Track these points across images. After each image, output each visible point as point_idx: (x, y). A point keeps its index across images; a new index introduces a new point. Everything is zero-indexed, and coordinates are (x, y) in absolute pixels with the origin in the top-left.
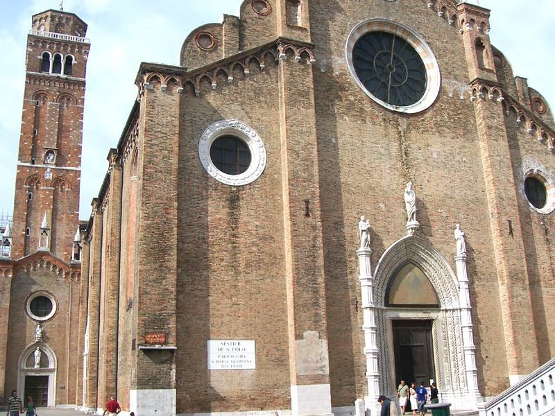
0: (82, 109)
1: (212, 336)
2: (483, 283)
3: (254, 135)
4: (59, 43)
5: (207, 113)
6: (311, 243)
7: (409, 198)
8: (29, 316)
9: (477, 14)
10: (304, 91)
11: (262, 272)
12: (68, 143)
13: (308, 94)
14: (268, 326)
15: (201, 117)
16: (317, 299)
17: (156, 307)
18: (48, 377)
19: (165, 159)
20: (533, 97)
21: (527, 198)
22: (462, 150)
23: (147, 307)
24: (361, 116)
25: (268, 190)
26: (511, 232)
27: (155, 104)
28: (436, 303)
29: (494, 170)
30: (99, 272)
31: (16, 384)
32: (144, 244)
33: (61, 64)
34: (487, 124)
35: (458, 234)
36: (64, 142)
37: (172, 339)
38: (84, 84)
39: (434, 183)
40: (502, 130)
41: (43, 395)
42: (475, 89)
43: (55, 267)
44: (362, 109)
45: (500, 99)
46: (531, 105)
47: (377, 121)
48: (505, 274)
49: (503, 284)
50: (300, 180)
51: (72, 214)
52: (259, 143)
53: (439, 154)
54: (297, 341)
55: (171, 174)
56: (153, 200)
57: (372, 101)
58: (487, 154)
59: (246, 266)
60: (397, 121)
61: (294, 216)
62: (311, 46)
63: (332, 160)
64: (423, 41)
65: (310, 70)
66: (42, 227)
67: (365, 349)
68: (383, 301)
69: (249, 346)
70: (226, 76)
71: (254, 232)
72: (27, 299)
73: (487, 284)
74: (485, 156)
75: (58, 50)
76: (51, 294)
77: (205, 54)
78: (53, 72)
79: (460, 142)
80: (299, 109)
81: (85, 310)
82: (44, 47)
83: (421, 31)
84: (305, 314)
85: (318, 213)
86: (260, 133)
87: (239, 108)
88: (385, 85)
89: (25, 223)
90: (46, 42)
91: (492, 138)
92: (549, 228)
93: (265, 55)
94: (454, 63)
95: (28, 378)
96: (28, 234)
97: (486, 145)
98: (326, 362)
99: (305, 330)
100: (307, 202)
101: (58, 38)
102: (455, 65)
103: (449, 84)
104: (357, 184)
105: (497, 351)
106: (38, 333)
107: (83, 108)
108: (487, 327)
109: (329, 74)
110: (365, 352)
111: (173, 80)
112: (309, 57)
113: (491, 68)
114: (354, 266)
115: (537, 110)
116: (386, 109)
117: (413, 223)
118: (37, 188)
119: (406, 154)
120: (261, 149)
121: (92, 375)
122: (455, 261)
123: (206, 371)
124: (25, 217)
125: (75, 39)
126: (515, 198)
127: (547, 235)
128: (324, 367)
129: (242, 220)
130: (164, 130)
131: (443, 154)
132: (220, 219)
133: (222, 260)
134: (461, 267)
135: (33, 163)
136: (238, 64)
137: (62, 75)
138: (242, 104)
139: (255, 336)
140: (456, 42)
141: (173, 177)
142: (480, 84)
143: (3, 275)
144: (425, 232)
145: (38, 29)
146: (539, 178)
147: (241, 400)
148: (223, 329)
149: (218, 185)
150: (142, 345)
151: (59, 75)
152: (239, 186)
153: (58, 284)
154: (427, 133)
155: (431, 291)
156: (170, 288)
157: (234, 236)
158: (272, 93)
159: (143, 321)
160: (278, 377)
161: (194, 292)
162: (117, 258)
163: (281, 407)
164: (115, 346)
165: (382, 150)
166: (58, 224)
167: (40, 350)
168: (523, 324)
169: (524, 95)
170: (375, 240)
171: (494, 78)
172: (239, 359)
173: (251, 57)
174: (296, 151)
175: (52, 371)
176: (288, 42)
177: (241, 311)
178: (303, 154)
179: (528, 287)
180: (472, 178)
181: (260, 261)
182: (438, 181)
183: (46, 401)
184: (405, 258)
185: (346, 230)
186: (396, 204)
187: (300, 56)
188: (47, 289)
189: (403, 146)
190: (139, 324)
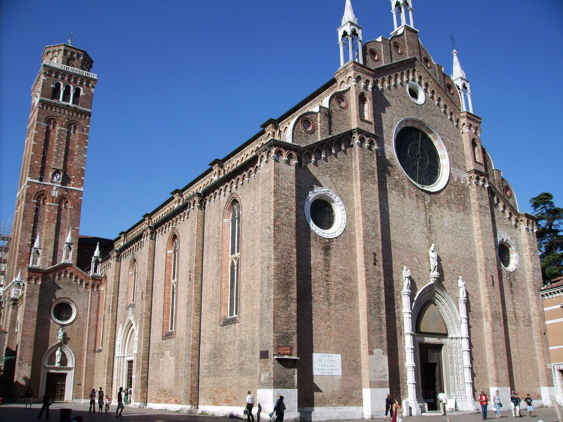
1: (314, 350)
2: (474, 320)
3: (338, 201)
4: (70, 75)
5: (309, 181)
6: (377, 285)
7: (433, 255)
8: (53, 320)
9: (473, 120)
11: (345, 304)
13: (373, 172)
14: (348, 344)
15: (305, 184)
16: (381, 326)
17: (285, 327)
18: (66, 374)
19: (288, 215)
20: (504, 185)
23: (279, 327)
24: (403, 192)
25: (348, 243)
26: (493, 284)
27: (280, 172)
28: (444, 332)
29: (483, 238)
30: (151, 288)
32: (276, 279)
33: (60, 91)
34: (479, 204)
35: (461, 283)
36: (69, 164)
37: (295, 351)
41: (62, 390)
42: (471, 177)
43: (77, 278)
44: (403, 186)
45: (487, 186)
46: (503, 191)
48: (489, 314)
49: (487, 321)
50: (370, 237)
52: (341, 207)
54: (370, 356)
55: (291, 227)
56: (280, 246)
58: (478, 226)
59: (336, 298)
60: (424, 197)
62: (375, 137)
63: (386, 223)
65: (375, 155)
66: (68, 242)
67: (406, 363)
69: (338, 358)
71: (340, 274)
73: (477, 321)
74: (476, 227)
75: (69, 80)
76: (72, 301)
78: (63, 100)
79: (461, 215)
80: (369, 184)
81: (114, 318)
82: (56, 77)
83: (438, 130)
85: (381, 263)
86: (342, 199)
87: (328, 179)
88: (415, 168)
89: (31, 234)
90: (59, 73)
91: (482, 214)
92: (512, 282)
97: (478, 219)
99: (374, 348)
100: (375, 255)
101: (70, 70)
103: (454, 171)
106: (60, 335)
110: (406, 366)
112: (374, 145)
113: (481, 162)
115: (506, 195)
116: (418, 187)
117: (435, 274)
118: (44, 204)
119: (430, 222)
120: (343, 212)
122: (458, 303)
123: (311, 376)
124: (31, 229)
125: (84, 73)
127: (511, 287)
128: (386, 375)
129: (333, 263)
131: (452, 223)
132: (319, 262)
133: (320, 293)
134: (462, 307)
136: (328, 145)
137: (70, 103)
138: (330, 176)
139: (341, 351)
140: (459, 139)
142: (475, 173)
143: (33, 282)
145: (51, 59)
147: (332, 398)
148: (322, 345)
149: (317, 237)
150: (276, 355)
151: (68, 103)
152: (330, 239)
153: (79, 293)
155: (443, 323)
156: (293, 313)
157: (327, 276)
158: (349, 169)
159: (276, 337)
160: (355, 382)
162: (200, 282)
163: (357, 404)
164: (197, 353)
165: (415, 218)
166: (60, 237)
167: (61, 351)
168: (500, 351)
169: (499, 183)
170: (413, 287)
171: (483, 169)
172: (332, 368)
175: (70, 369)
176: (362, 132)
179: (503, 324)
180: (468, 242)
181: (343, 296)
182: (449, 243)
183: (64, 395)
185: (394, 276)
186: (424, 259)
187: (369, 144)
189: (428, 216)
190: (274, 339)
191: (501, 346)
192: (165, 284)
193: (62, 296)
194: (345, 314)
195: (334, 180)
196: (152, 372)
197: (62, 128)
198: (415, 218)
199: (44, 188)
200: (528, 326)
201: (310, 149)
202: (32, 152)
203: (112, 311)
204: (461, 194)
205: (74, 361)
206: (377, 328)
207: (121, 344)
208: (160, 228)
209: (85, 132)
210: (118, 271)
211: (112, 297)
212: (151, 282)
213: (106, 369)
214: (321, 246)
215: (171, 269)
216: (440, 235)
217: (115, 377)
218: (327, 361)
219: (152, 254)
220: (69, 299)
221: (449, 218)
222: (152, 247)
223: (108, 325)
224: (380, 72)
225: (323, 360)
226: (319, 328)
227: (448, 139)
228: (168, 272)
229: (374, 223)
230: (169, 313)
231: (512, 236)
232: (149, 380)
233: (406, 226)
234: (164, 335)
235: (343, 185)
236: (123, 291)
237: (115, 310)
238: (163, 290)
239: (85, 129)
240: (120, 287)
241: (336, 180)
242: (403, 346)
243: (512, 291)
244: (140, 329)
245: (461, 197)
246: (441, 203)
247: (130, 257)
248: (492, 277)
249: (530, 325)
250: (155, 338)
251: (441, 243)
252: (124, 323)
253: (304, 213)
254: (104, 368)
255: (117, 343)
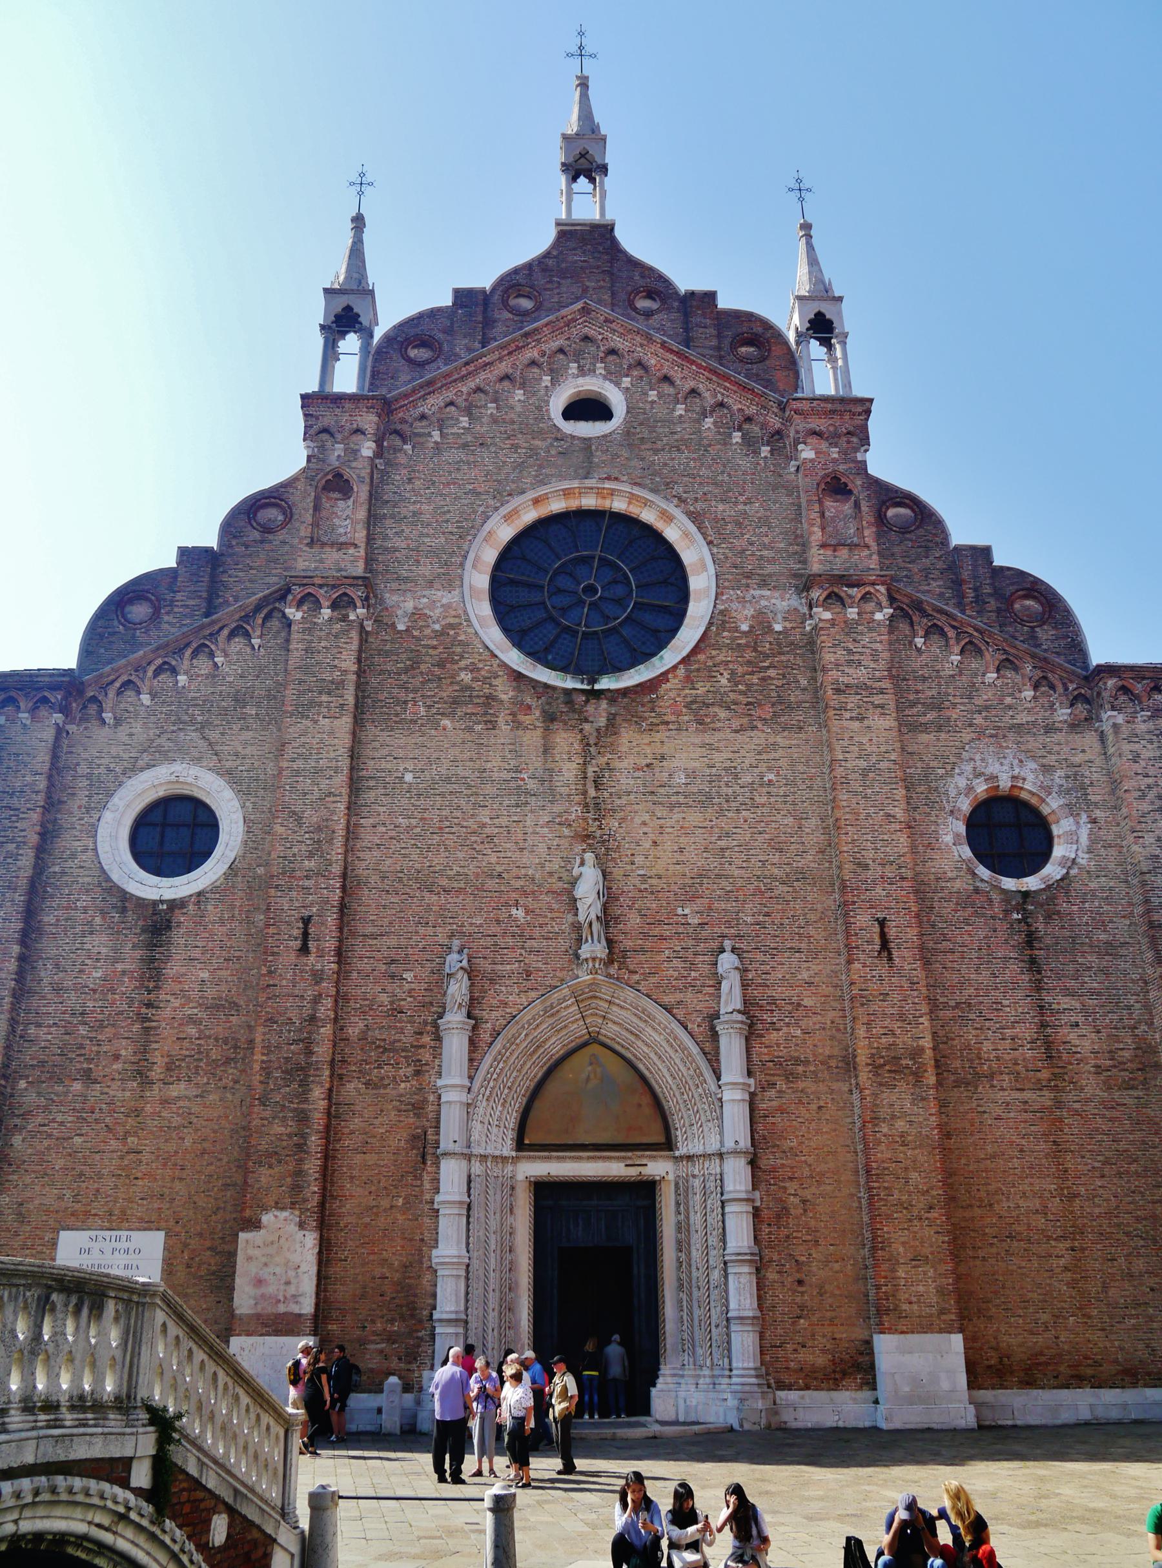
5: (126, 756)
6: (306, 1012)
10: (332, 682)
13: (341, 684)
15: (112, 766)
16: (304, 1136)
19: (9, 860)
21: (967, 852)
22: (764, 756)
24: (486, 713)
28: (662, 1139)
39: (669, 846)
40: (882, 692)
44: (490, 698)
47: (526, 719)
53: (692, 775)
57: (518, 677)
61: (273, 954)
63: (401, 820)
64: (677, 513)
65: (354, 634)
68: (511, 1135)
70: (174, 671)
77: (134, 636)
79: (758, 738)
80: (316, 722)
84: (271, 1171)
92: (1041, 927)
93: (267, 618)
94: (765, 547)
98: (308, 1285)
99: (265, 1209)
100: (306, 921)
102: (765, 553)
103: (742, 601)
104: (456, 868)
105: (837, 1266)
108: (804, 1202)
109: (416, 633)
111: (45, 700)
114: (426, 1056)
126: (908, 859)
127: (1031, 947)
129: (173, 969)
130: (15, 802)
132: (124, 972)
133: (117, 1057)
141: (19, 898)
144: (631, 967)
146: (1024, 795)
154: (661, 727)
155: (648, 1110)
157: (149, 1005)
161: (45, 1128)
165: (532, 785)
173: (234, 625)
174: (294, 813)
176: (305, 581)
177: (143, 1168)
178: (311, 817)
184: (577, 1031)
186: (555, 906)
189: (590, 770)
191: (914, 1175)
194: (195, 1109)
195: (214, 735)
198: (532, 785)
200: (1133, 1088)
201: (136, 671)
204: (768, 668)
206: (285, 1144)
214: (140, 923)
216: (646, 817)
218: (108, 1251)
221: (697, 755)
224: (429, 393)
225: (95, 1253)
226: (97, 1157)
227: (721, 507)
229: (319, 829)
231: (1051, 760)
233: (484, 816)
235: (245, 744)
241: (222, 734)
242: (427, 1197)
243: (1033, 961)
245: (763, 679)
246: (659, 715)
248: (882, 923)
249: (1145, 1082)
251: (647, 844)
253: (95, 843)
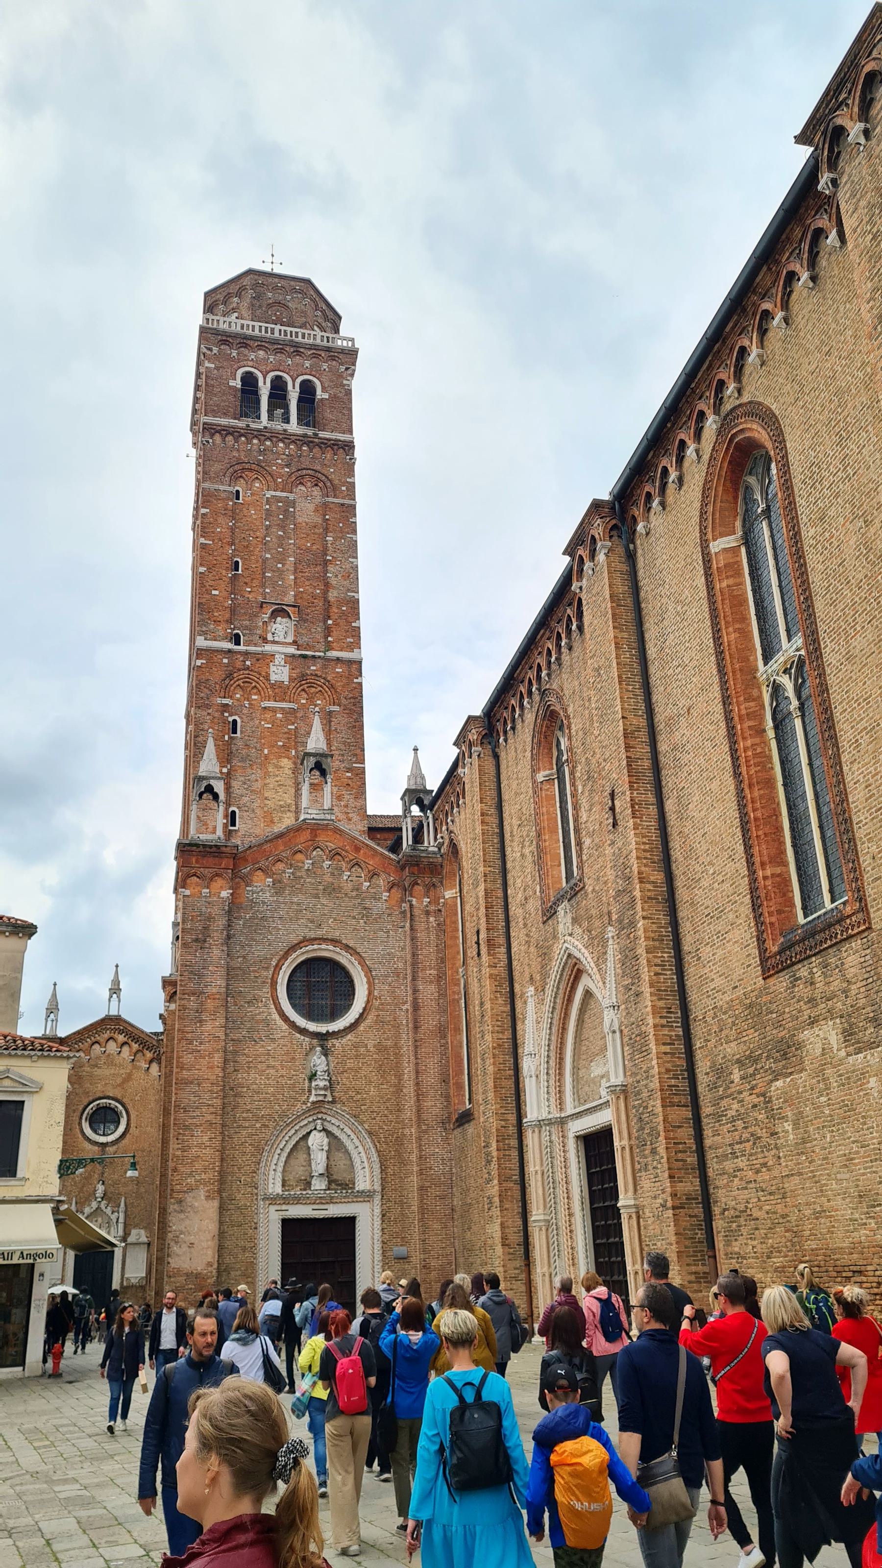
0: (351, 510)
4: (278, 347)
12: (325, 593)
30: (647, 763)
31: (253, 1248)
38: (349, 447)
51: (349, 770)
72: (278, 967)
76: (347, 948)
81: (502, 969)
95: (287, 1224)
96: (233, 824)
107: (354, 507)
121: (681, 1187)
135: (238, 643)
151: (286, 426)
167: (329, 1133)
188: (336, 934)
192: (726, 700)
193: (312, 935)
196: (729, 1165)
197: (278, 494)
199: (248, 663)
202: (201, 565)
203: (490, 942)
205: (377, 1167)
207: (543, 1071)
208: (648, 488)
209: (343, 498)
210: (494, 793)
211: (482, 894)
212: (644, 736)
213: (496, 1182)
215: (744, 619)
217: (537, 1214)
219: (628, 616)
220: (335, 942)
222: (622, 588)
223: (482, 1004)
228: (729, 637)
230: (779, 829)
232: (716, 1210)
234: (775, 949)
236: (523, 855)
237: (502, 940)
238: (723, 731)
239: (344, 488)
240: (508, 850)
244: (628, 959)
247: (530, 717)
250: (719, 982)
252: (545, 976)
254: (489, 1181)
255: (528, 1065)
